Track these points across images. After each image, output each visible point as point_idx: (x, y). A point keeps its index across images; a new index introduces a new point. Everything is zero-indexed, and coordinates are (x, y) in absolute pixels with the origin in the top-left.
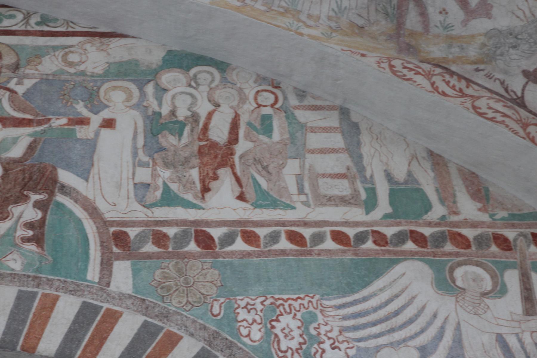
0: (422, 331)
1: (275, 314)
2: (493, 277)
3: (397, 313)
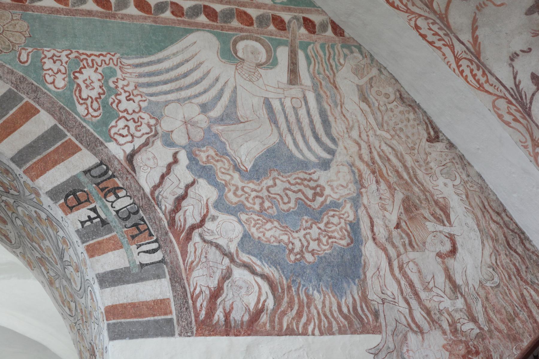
0: (205, 92)
1: (79, 66)
2: (268, 51)
3: (185, 75)
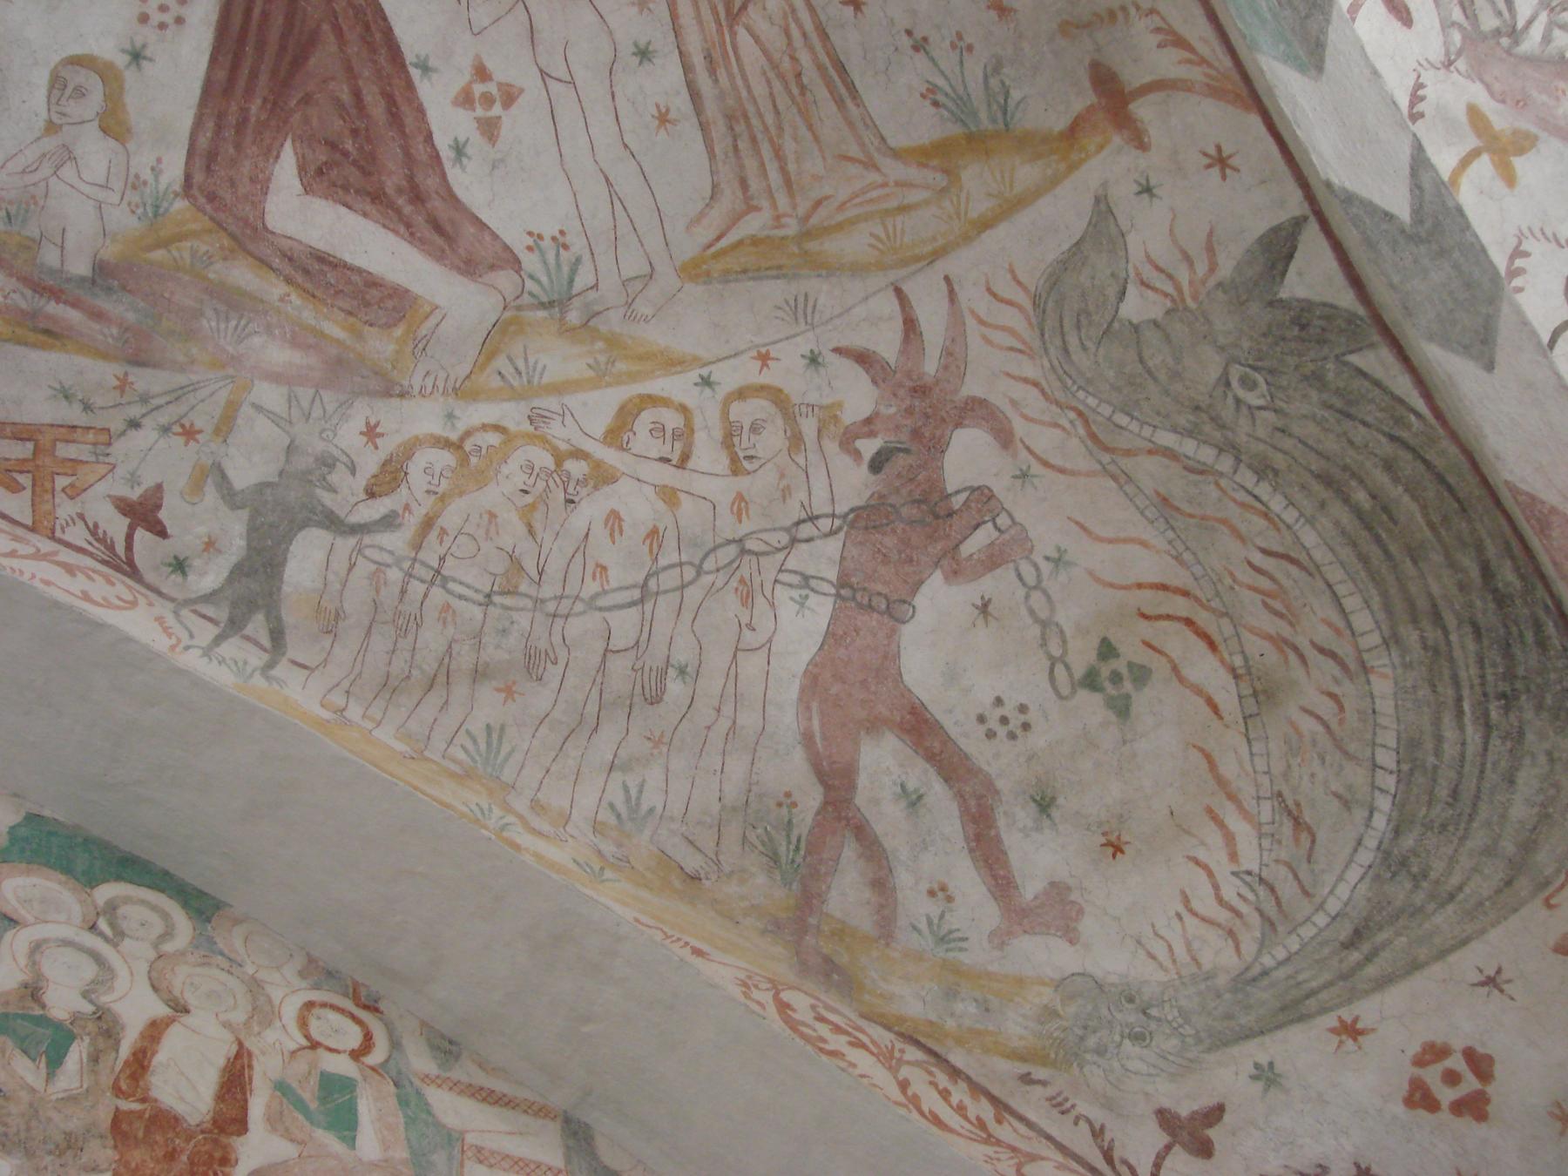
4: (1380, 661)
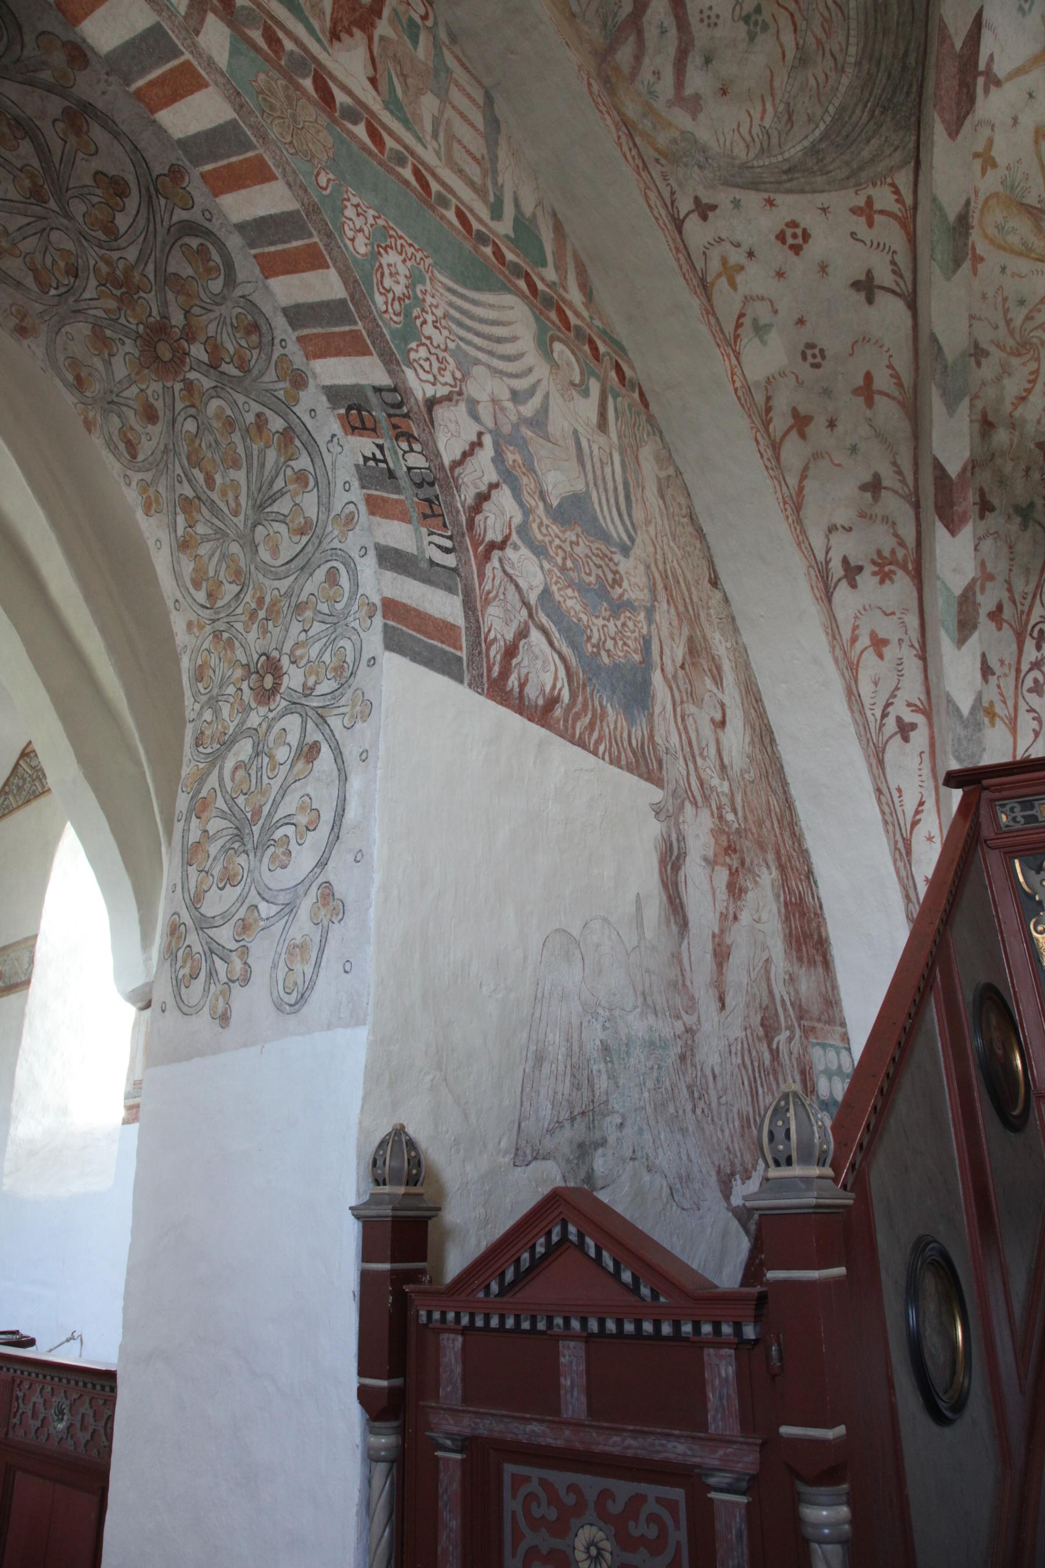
2: (582, 374)
4: (850, 70)
